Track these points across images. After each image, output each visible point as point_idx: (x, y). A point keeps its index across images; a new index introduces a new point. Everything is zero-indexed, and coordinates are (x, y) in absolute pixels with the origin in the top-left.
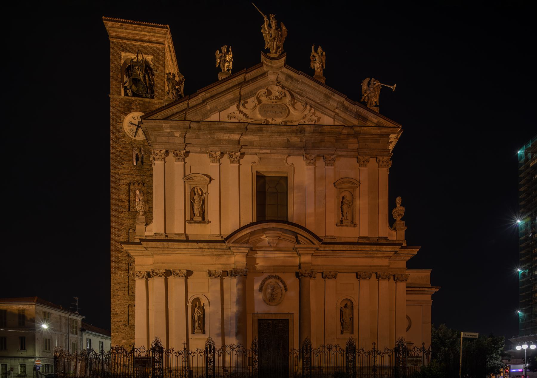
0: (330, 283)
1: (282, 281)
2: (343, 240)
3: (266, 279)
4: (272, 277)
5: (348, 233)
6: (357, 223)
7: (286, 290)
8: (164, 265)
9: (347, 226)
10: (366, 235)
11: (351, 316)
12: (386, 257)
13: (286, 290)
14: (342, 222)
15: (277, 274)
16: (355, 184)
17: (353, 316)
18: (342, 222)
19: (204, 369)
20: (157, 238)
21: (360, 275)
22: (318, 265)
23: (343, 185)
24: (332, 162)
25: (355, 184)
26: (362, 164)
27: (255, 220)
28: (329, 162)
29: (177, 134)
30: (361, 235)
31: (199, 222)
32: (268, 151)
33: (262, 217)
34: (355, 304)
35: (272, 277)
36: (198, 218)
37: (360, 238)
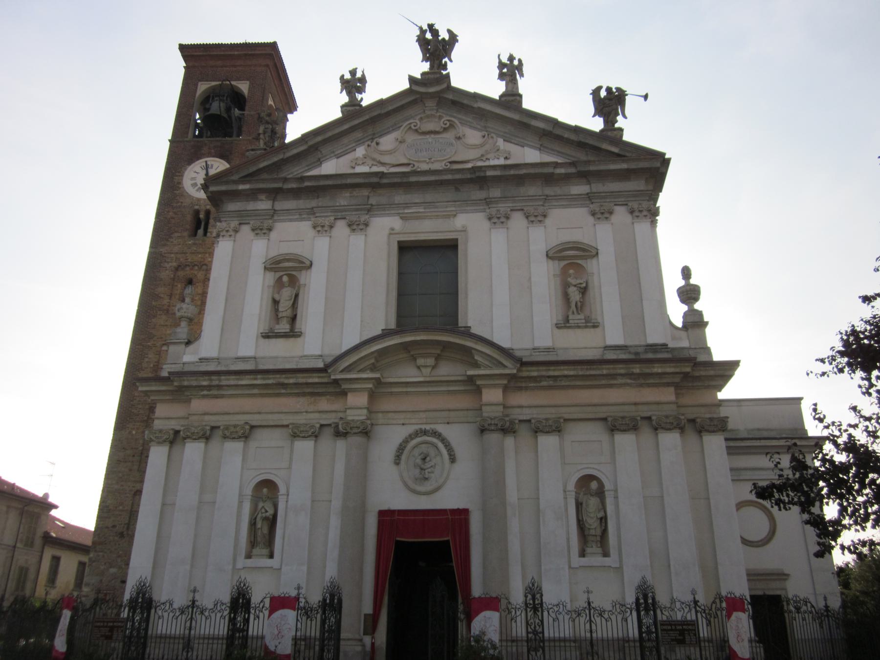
0: (548, 442)
1: (443, 440)
3: (411, 437)
5: (580, 344)
6: (600, 320)
7: (453, 459)
8: (207, 418)
9: (579, 327)
10: (620, 341)
11: (601, 514)
12: (668, 385)
13: (453, 459)
14: (567, 320)
15: (432, 426)
16: (588, 252)
17: (605, 512)
18: (567, 320)
19: (317, 643)
20: (204, 368)
21: (615, 426)
24: (540, 218)
25: (588, 252)
26: (603, 215)
27: (392, 325)
28: (536, 218)
30: (610, 342)
31: (285, 336)
33: (405, 318)
34: (608, 486)
35: (425, 433)
36: (284, 327)
37: (607, 348)
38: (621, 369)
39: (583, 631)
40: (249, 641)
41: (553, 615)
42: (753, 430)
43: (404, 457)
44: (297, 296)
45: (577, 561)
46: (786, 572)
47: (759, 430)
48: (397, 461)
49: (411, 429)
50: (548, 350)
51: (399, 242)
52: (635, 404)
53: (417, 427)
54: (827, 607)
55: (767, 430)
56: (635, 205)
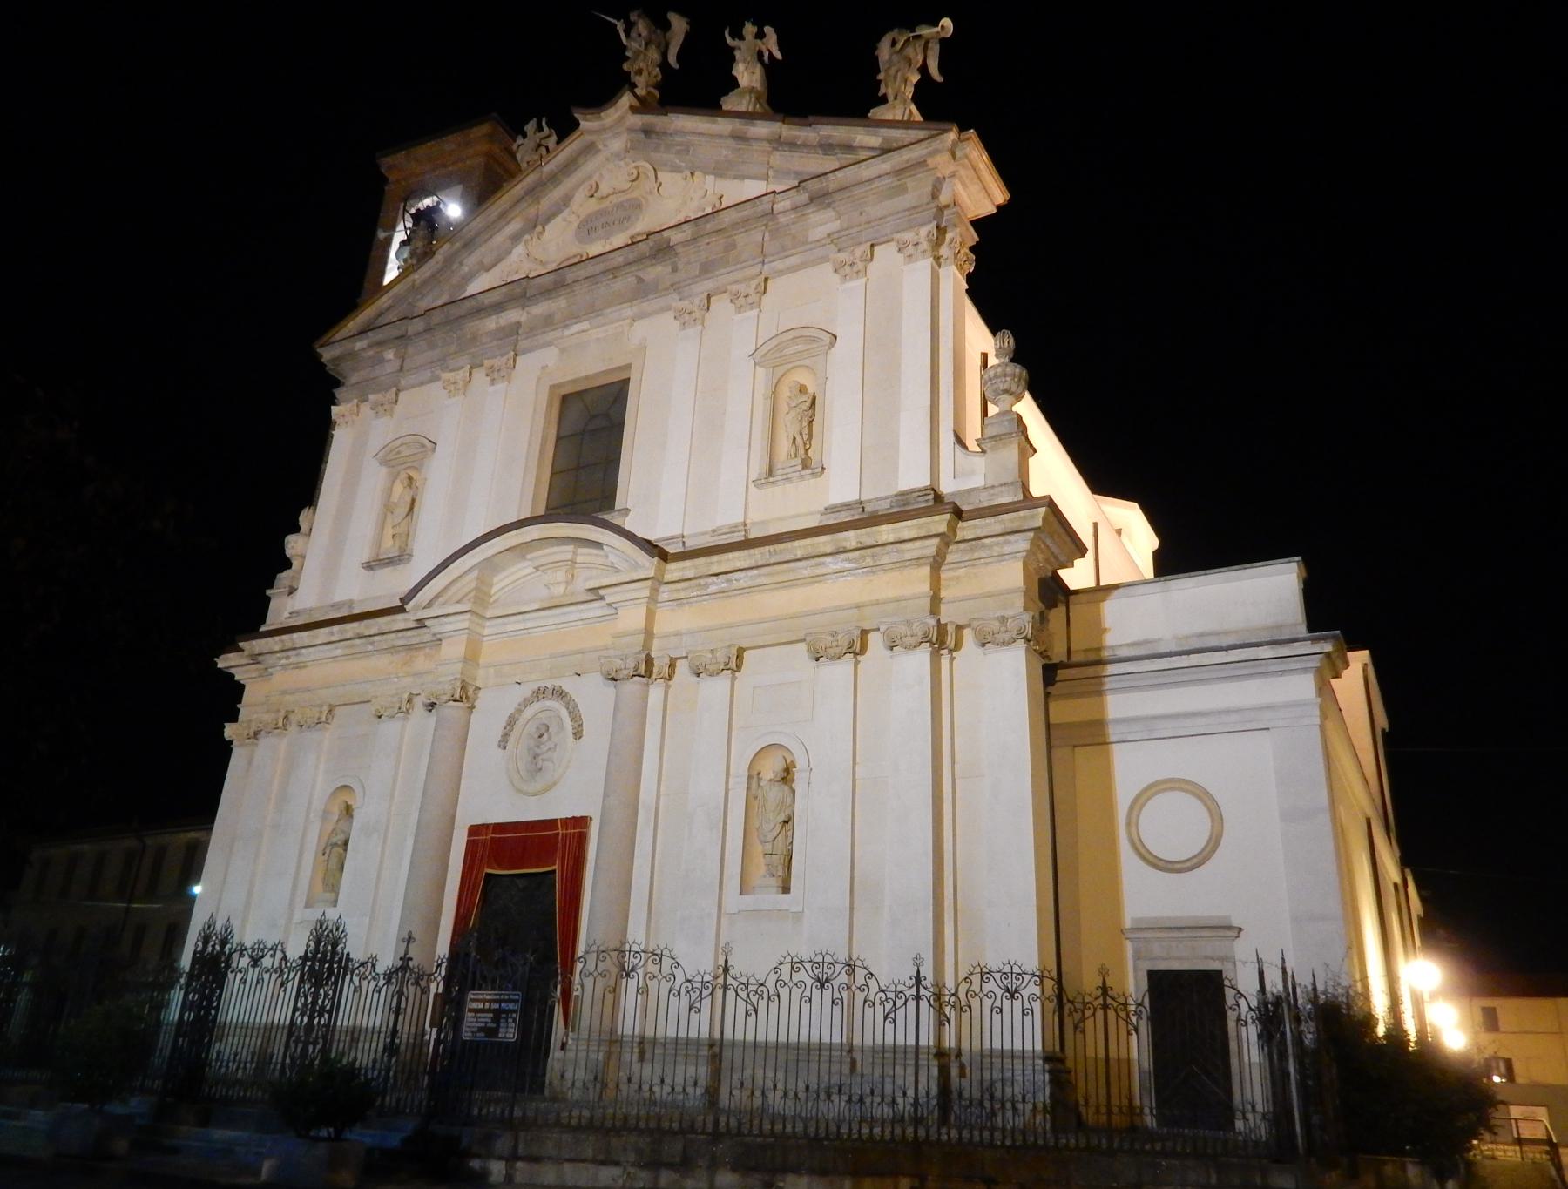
2: (773, 530)
3: (527, 703)
4: (540, 693)
7: (578, 735)
8: (288, 698)
10: (852, 496)
15: (557, 683)
22: (678, 634)
23: (787, 351)
29: (389, 355)
32: (585, 325)
38: (824, 543)
39: (700, 1028)
40: (727, 1054)
41: (356, 979)
42: (1187, 637)
43: (512, 739)
44: (413, 501)
45: (733, 900)
46: (1236, 923)
47: (1201, 635)
48: (503, 743)
49: (526, 691)
50: (733, 528)
51: (553, 387)
52: (858, 607)
53: (535, 687)
54: (1105, 989)
55: (1217, 634)
56: (909, 236)
